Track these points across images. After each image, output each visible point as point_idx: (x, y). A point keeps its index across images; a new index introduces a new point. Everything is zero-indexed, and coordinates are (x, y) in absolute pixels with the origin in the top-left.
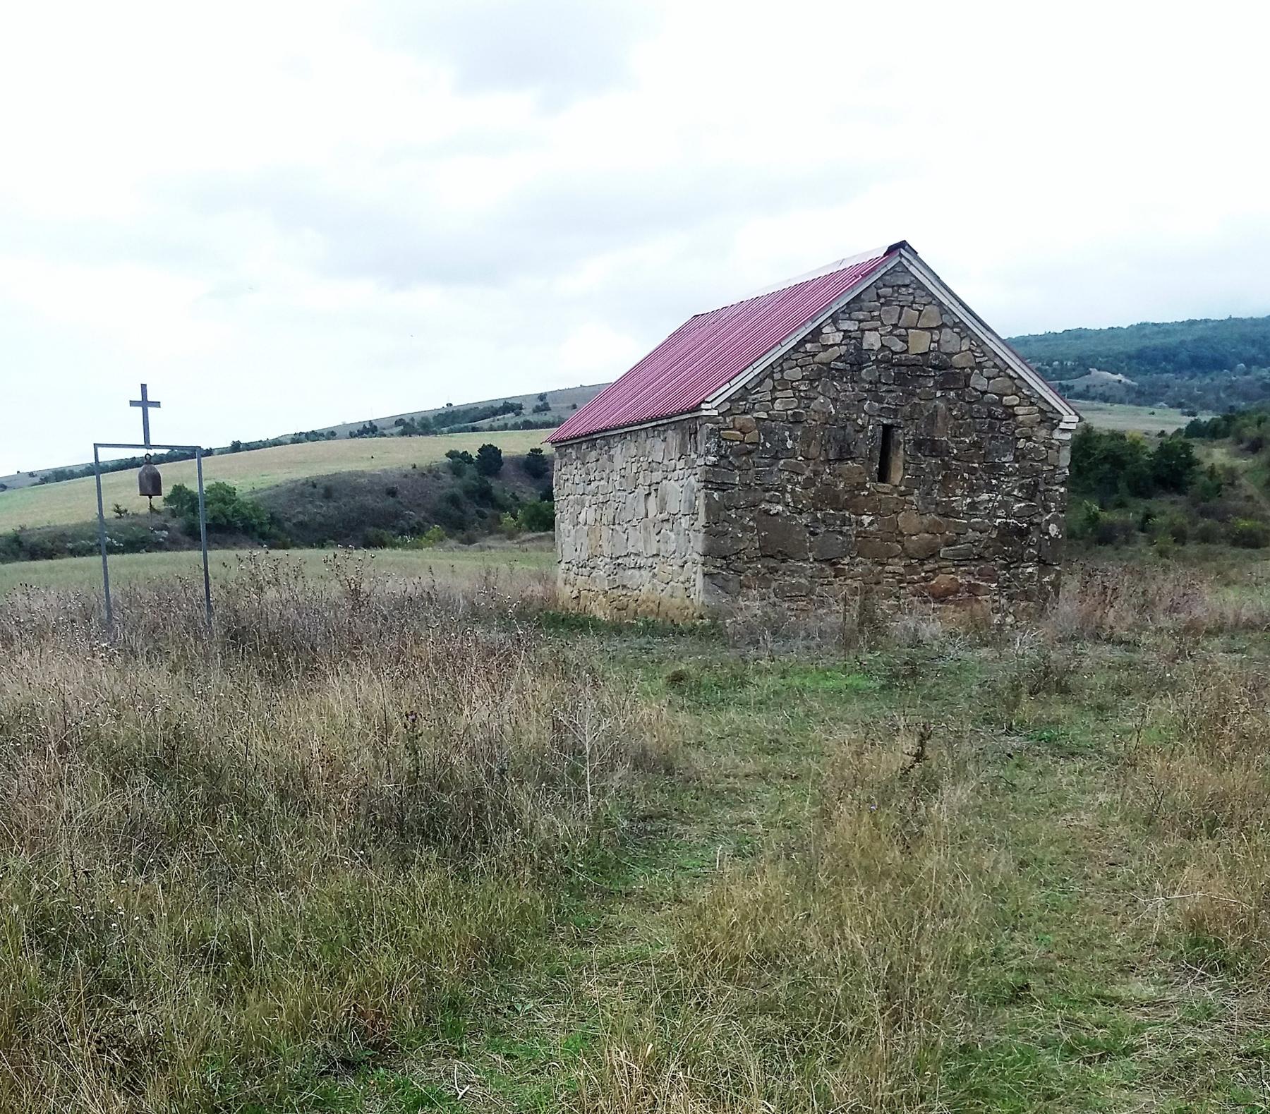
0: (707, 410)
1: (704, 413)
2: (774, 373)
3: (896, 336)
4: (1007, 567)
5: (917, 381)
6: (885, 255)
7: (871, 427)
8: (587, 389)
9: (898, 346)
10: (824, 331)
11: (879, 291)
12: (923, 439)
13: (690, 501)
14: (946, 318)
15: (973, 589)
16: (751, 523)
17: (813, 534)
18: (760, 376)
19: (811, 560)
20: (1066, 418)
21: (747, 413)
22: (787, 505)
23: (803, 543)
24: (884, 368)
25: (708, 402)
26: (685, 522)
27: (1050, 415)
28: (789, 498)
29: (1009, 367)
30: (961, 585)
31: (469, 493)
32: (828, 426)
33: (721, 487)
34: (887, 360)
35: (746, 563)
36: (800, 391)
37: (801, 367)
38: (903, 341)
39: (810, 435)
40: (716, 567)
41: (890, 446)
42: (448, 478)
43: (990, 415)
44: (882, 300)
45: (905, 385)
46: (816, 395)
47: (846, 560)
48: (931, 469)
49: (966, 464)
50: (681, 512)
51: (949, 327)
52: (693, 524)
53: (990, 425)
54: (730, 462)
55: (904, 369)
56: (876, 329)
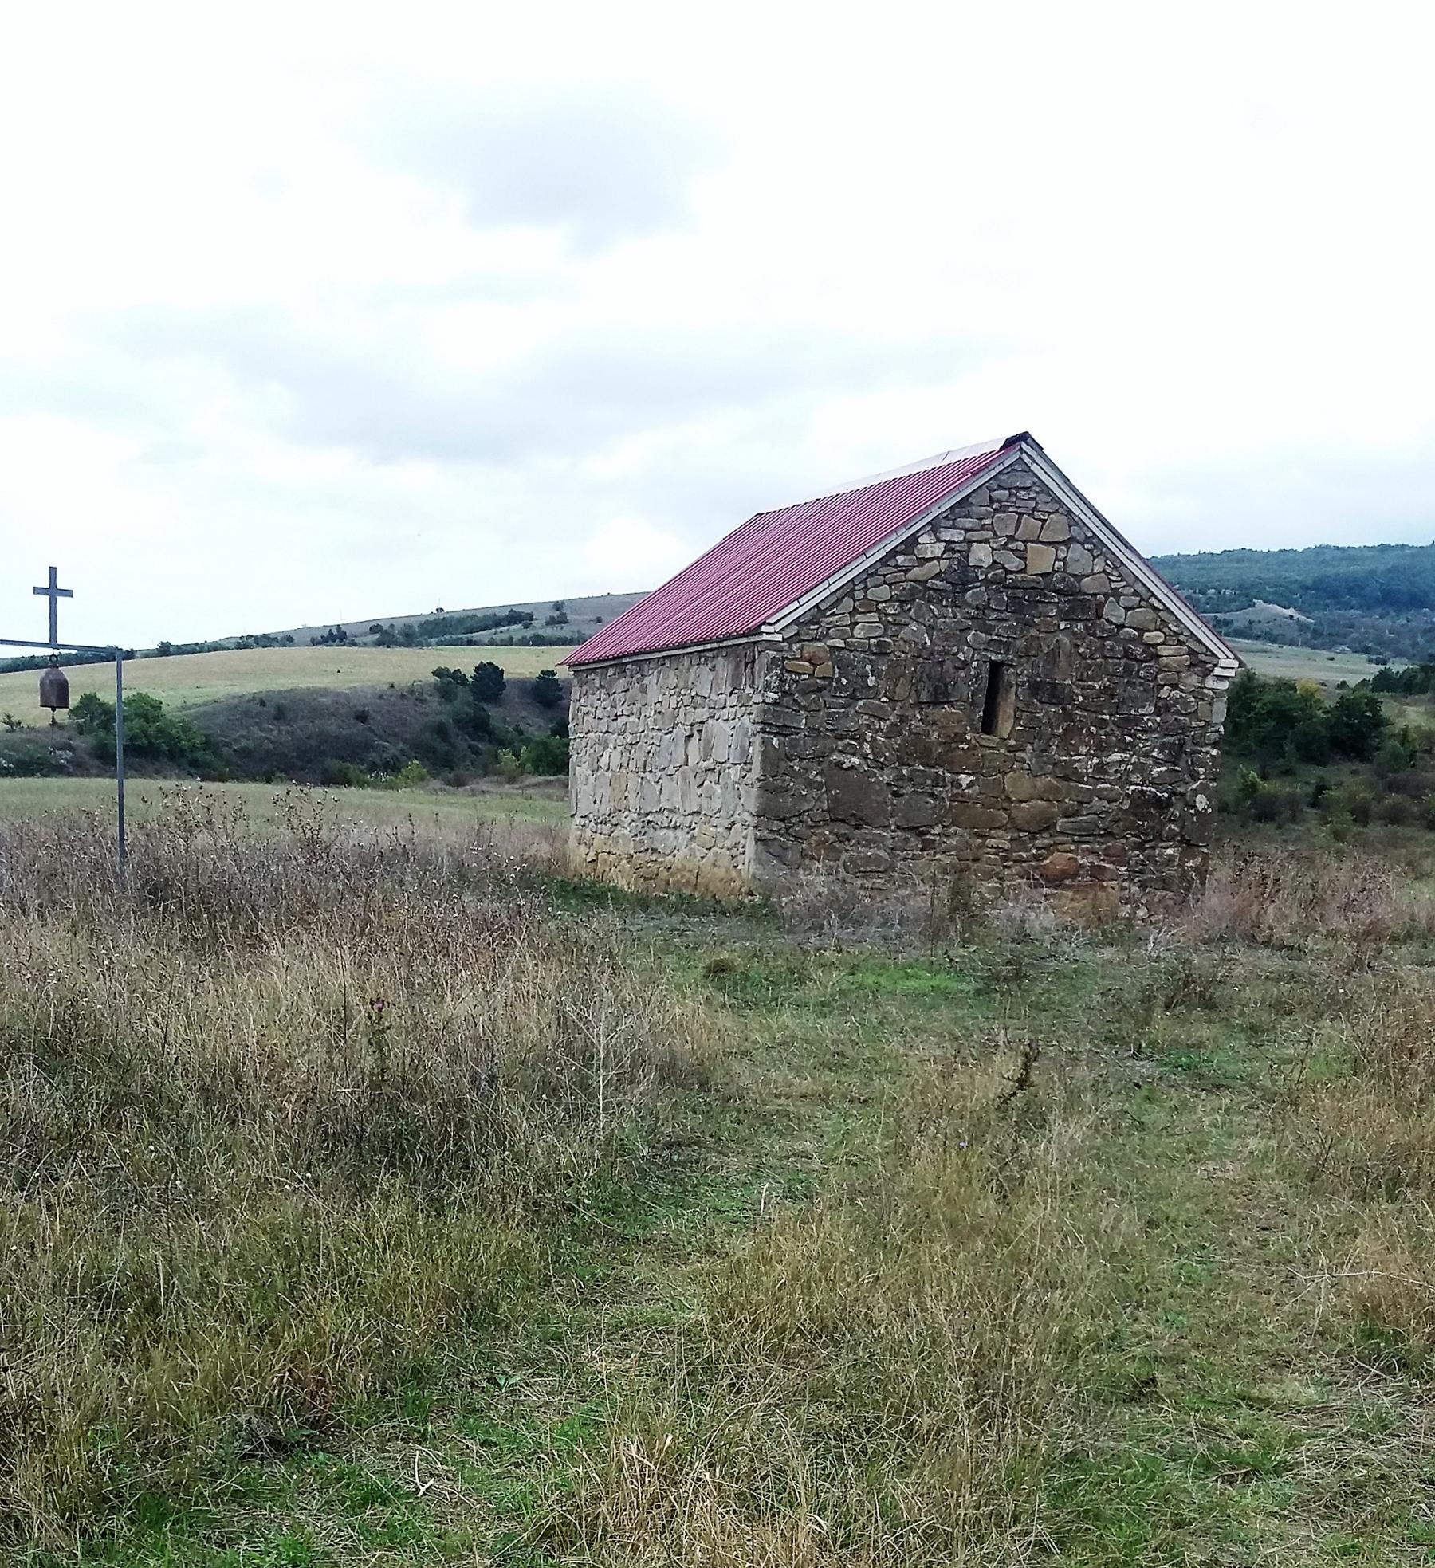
0: (768, 633)
1: (765, 637)
3: (1012, 550)
4: (1140, 846)
6: (1002, 448)
7: (975, 664)
8: (617, 599)
9: (1014, 563)
10: (920, 540)
11: (993, 494)
13: (742, 747)
15: (1097, 873)
16: (819, 778)
17: (896, 794)
18: (838, 594)
19: (893, 827)
20: (1223, 662)
21: (819, 640)
22: (865, 757)
24: (995, 590)
25: (770, 624)
26: (734, 773)
27: (1202, 657)
28: (867, 747)
29: (1153, 595)
30: (1082, 866)
31: (461, 722)
32: (921, 660)
34: (999, 581)
36: (887, 615)
37: (890, 585)
39: (899, 670)
40: (771, 831)
41: (999, 689)
42: (434, 703)
43: (1127, 655)
46: (907, 620)
47: (937, 830)
48: (1049, 719)
49: (1094, 715)
50: (731, 761)
51: (1079, 542)
52: (745, 776)
53: (1126, 666)
54: (795, 701)
55: (1019, 593)
56: (987, 541)
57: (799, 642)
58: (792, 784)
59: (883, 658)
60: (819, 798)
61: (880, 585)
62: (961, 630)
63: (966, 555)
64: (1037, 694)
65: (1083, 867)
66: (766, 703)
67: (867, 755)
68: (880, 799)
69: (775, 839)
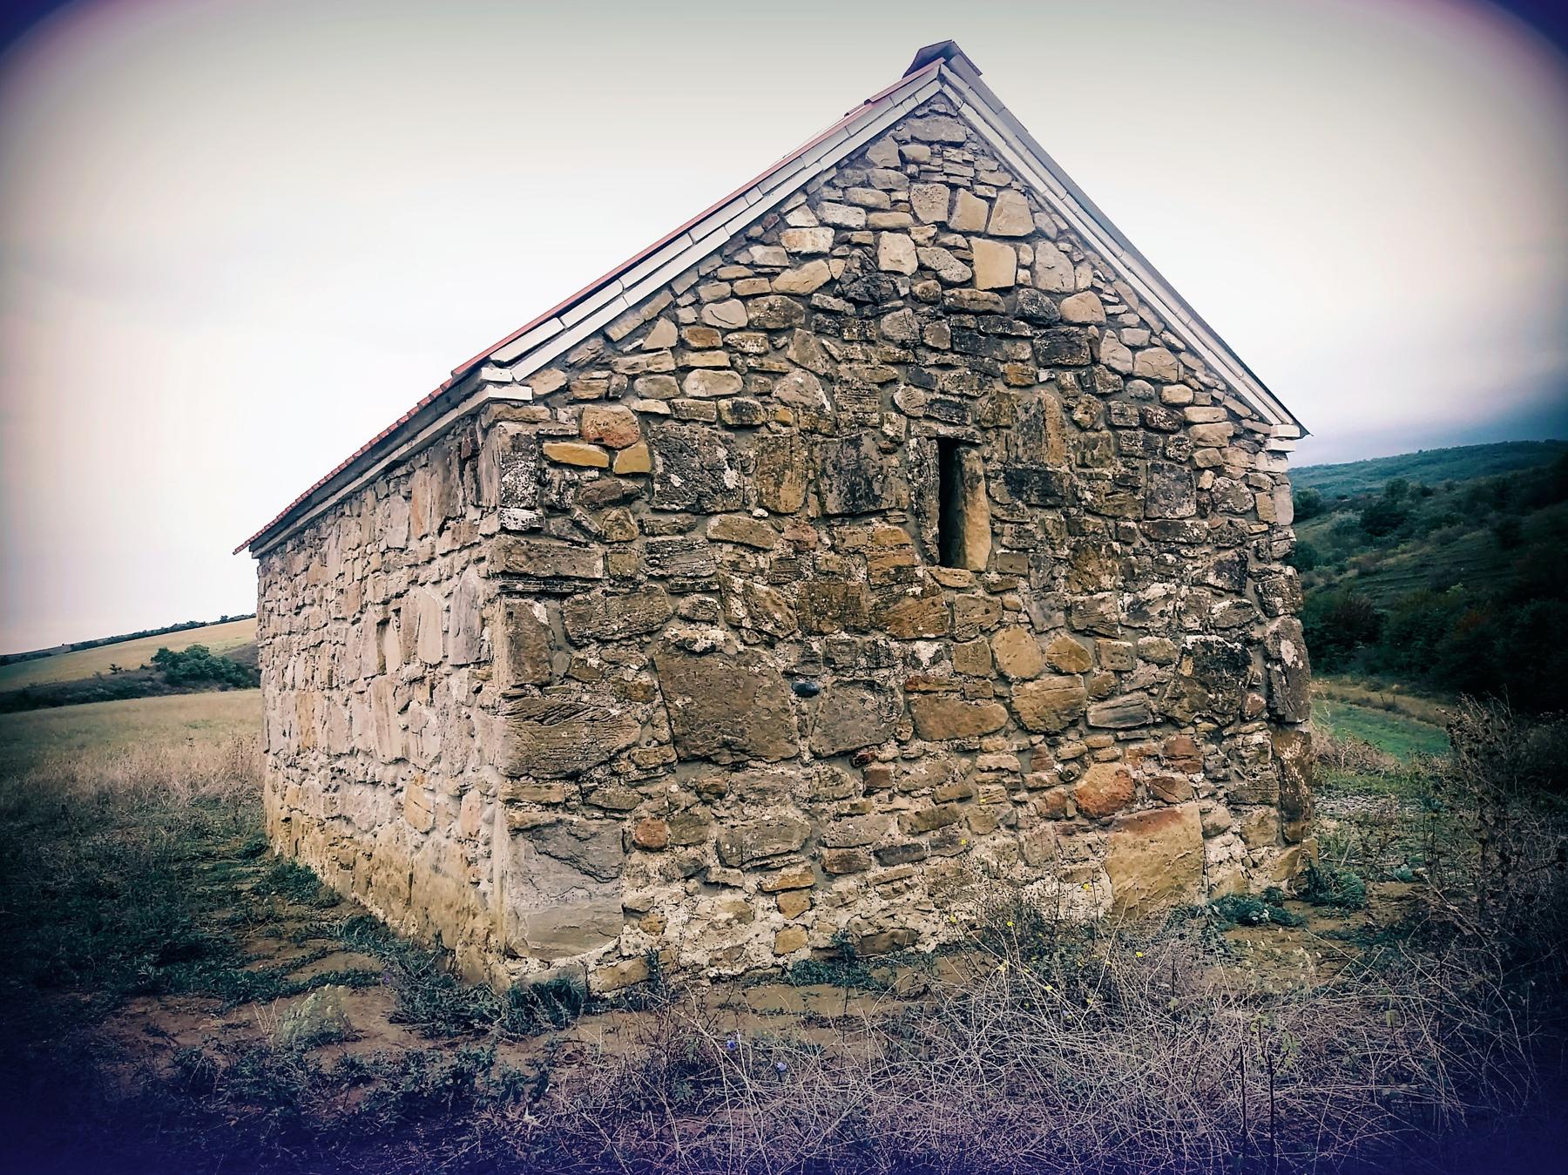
2: (677, 306)
4: (1216, 736)
5: (1000, 344)
7: (913, 442)
10: (790, 220)
11: (906, 149)
12: (1024, 470)
14: (1043, 221)
15: (1160, 793)
16: (645, 678)
17: (805, 693)
22: (736, 627)
23: (784, 717)
27: (1247, 424)
28: (738, 608)
30: (1137, 783)
32: (819, 438)
33: (553, 588)
35: (639, 783)
36: (744, 354)
37: (744, 299)
38: (962, 260)
39: (780, 457)
44: (912, 169)
45: (974, 354)
47: (890, 750)
48: (1046, 532)
50: (450, 660)
53: (1146, 442)
54: (577, 524)
55: (970, 321)
56: (904, 230)
57: (571, 403)
58: (586, 698)
59: (751, 436)
60: (650, 718)
61: (726, 299)
62: (881, 385)
63: (871, 253)
64: (1022, 491)
65: (1140, 784)
66: (508, 532)
67: (740, 621)
68: (775, 705)
69: (559, 821)
